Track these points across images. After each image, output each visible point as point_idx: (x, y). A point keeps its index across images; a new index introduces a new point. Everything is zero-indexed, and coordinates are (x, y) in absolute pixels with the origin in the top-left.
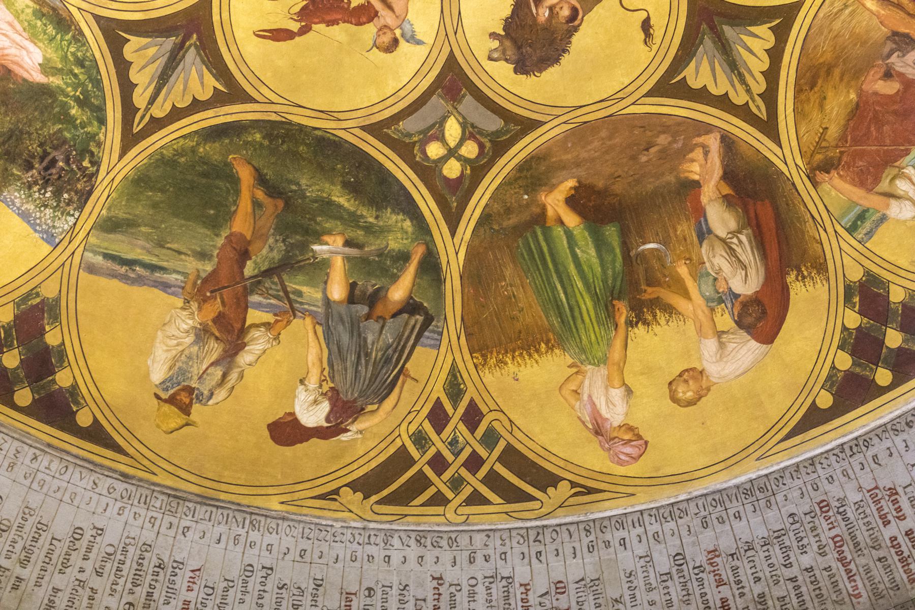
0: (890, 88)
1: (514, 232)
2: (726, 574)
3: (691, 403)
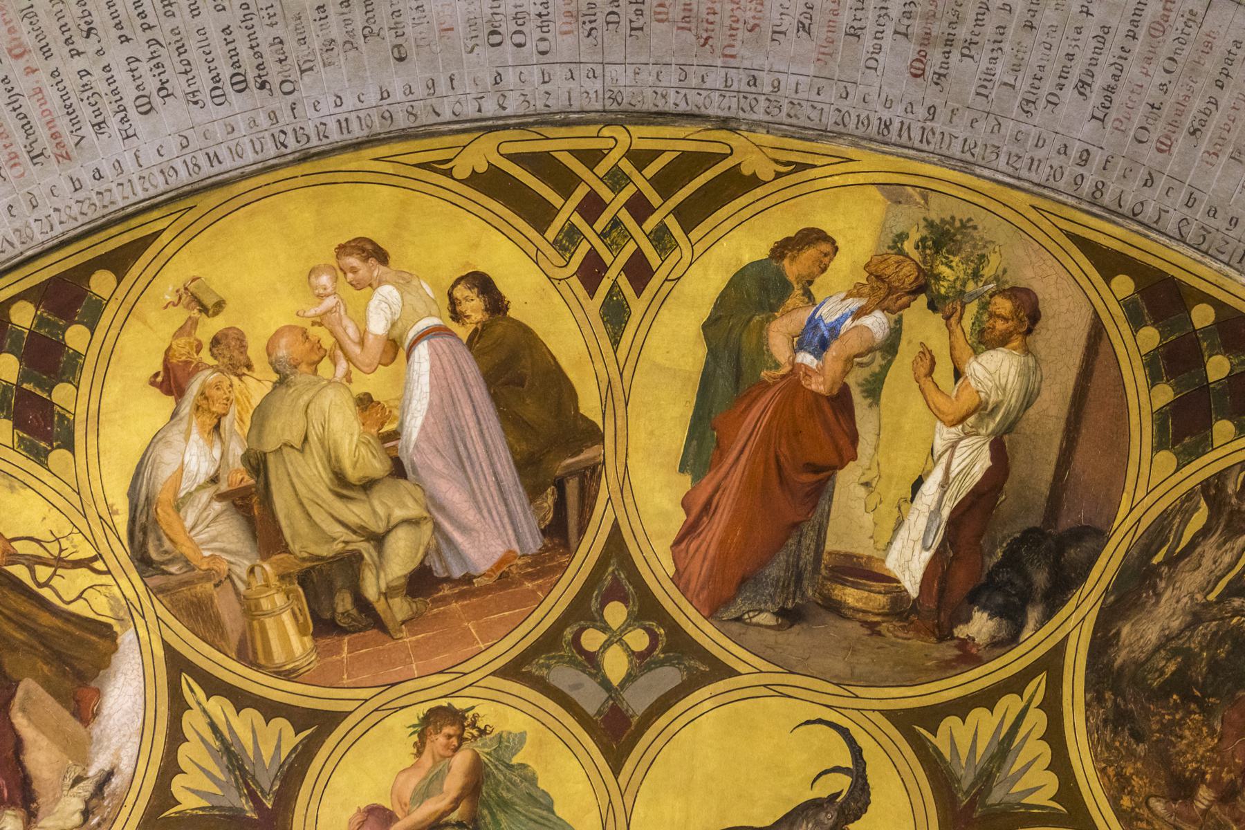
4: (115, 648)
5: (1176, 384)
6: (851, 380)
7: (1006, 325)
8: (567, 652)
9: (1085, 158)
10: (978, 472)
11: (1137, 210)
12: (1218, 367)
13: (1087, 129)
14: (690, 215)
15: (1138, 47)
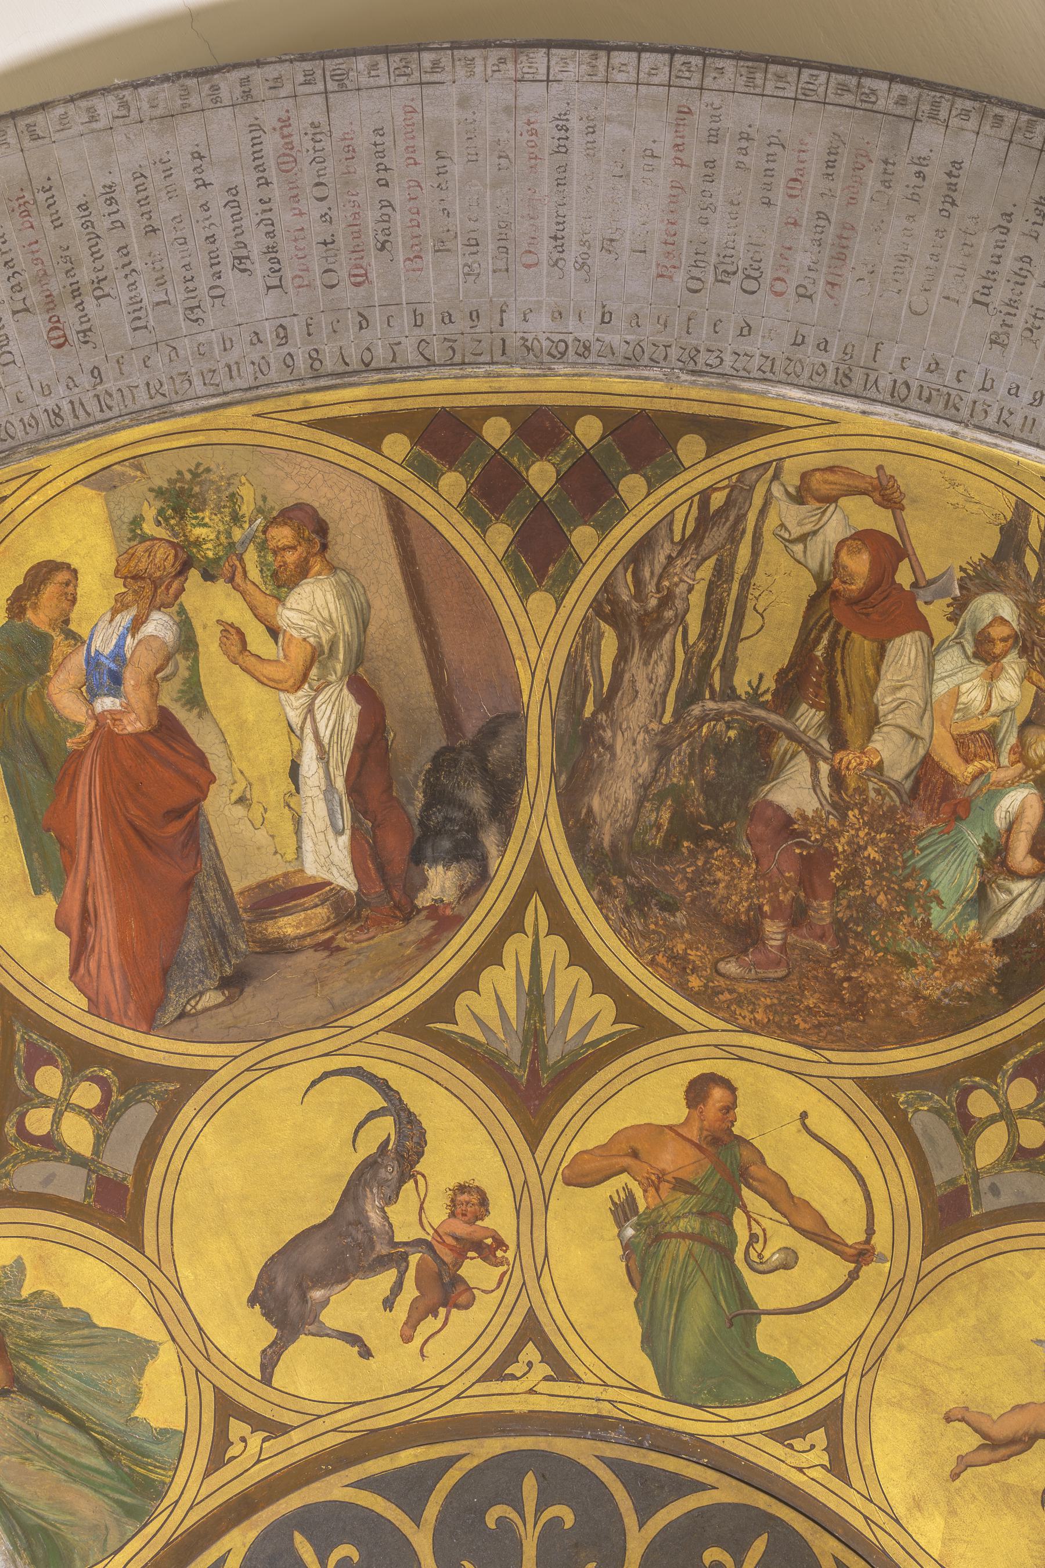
5: (508, 516)
6: (165, 700)
7: (296, 554)
8: (18, 1149)
9: (283, 335)
11: (367, 357)
12: (541, 476)
13: (269, 305)
15: (277, 192)
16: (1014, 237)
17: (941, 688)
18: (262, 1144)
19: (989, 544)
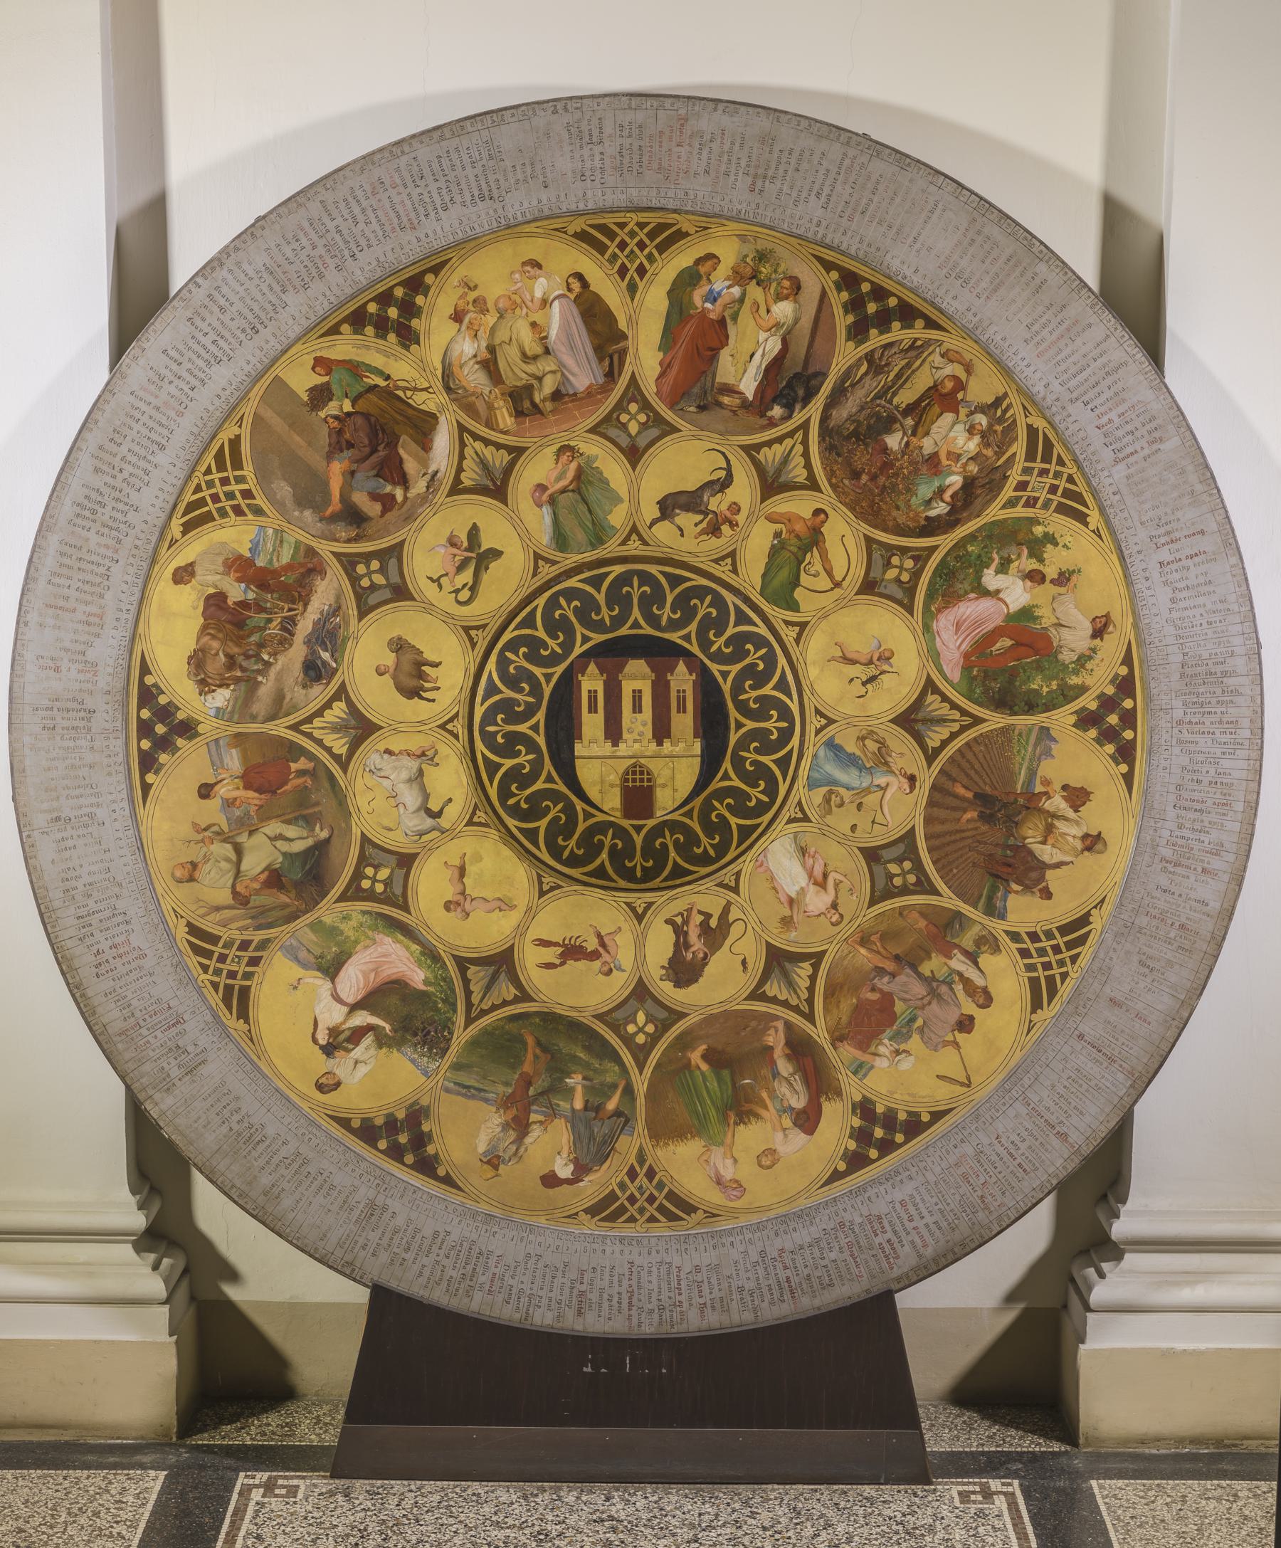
0: (874, 996)
1: (673, 1072)
2: (789, 1263)
3: (769, 1167)
4: (438, 423)
6: (726, 314)
9: (819, 224)
10: (776, 351)
12: (872, 308)
13: (820, 213)
14: (662, 248)
15: (841, 178)
16: (1050, 312)
17: (952, 434)
18: (684, 460)
19: (990, 400)
